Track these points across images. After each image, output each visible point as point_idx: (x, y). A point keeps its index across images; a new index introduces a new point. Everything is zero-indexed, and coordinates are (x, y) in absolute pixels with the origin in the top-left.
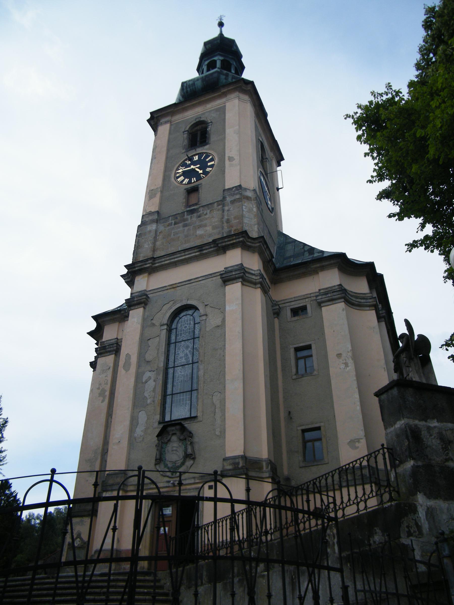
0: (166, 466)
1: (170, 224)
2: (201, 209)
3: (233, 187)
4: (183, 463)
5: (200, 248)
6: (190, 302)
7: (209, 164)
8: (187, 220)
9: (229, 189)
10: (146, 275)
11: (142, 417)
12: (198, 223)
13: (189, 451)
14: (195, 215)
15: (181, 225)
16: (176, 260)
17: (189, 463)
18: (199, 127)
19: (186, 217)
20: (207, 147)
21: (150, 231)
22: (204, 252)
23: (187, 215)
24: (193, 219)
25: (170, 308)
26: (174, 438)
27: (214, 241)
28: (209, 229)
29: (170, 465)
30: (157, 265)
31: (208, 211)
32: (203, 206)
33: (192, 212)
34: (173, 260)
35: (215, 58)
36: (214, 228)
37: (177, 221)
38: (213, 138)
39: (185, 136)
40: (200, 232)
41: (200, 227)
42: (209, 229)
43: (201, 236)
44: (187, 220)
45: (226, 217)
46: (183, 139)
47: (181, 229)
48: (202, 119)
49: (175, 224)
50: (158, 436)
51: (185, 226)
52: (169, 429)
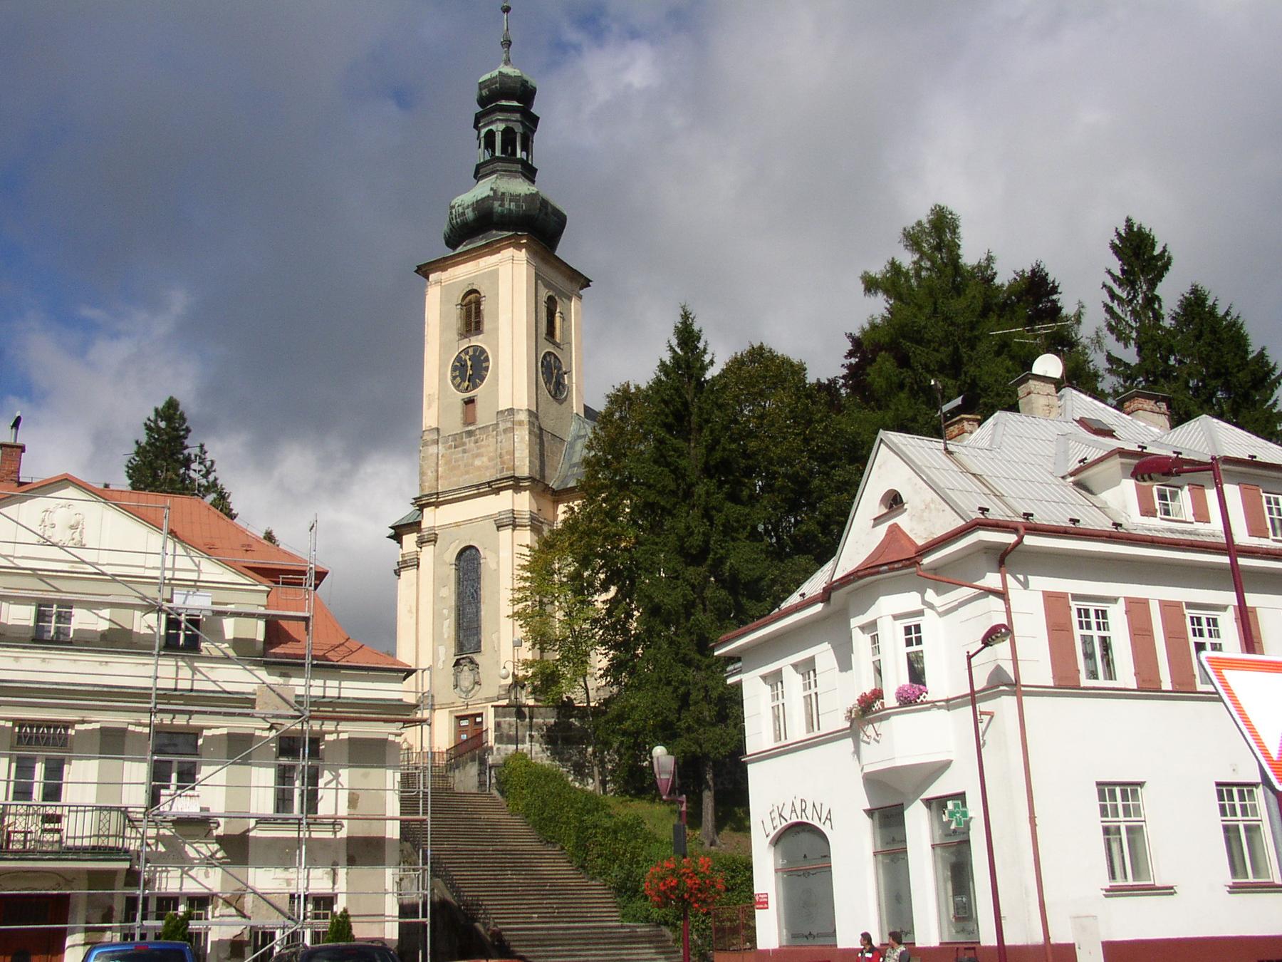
0: (461, 690)
1: (450, 447)
2: (478, 432)
3: (506, 410)
4: (473, 688)
5: (477, 486)
6: (471, 544)
7: (484, 365)
8: (464, 444)
9: (501, 411)
10: (433, 507)
11: (442, 650)
12: (475, 451)
13: (477, 680)
14: (473, 438)
15: (460, 449)
16: (458, 496)
17: (477, 687)
18: (472, 297)
19: (464, 440)
20: (480, 337)
21: (431, 455)
22: (482, 490)
23: (466, 438)
24: (470, 443)
25: (456, 548)
26: (466, 668)
27: (488, 483)
28: (485, 459)
29: (464, 690)
30: (441, 499)
31: (485, 436)
32: (479, 429)
33: (470, 433)
34: (455, 496)
35: (493, 127)
36: (490, 459)
37: (457, 443)
38: (487, 325)
39: (459, 311)
40: (477, 462)
41: (478, 456)
42: (485, 459)
43: (479, 468)
44: (464, 444)
45: (499, 451)
46: (455, 314)
47: (461, 455)
48: (474, 288)
49: (455, 448)
50: (454, 666)
51: (464, 451)
52: (461, 661)
